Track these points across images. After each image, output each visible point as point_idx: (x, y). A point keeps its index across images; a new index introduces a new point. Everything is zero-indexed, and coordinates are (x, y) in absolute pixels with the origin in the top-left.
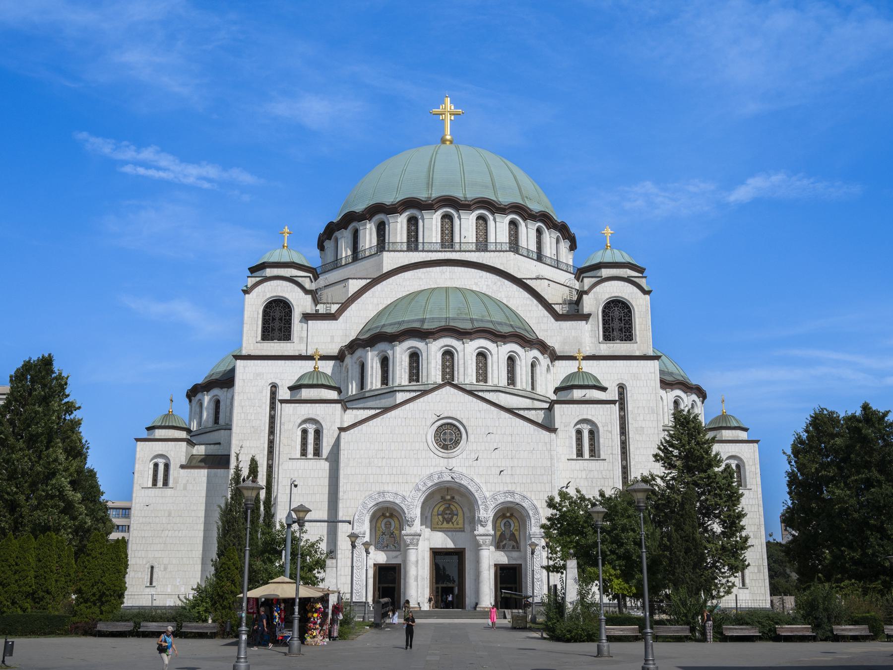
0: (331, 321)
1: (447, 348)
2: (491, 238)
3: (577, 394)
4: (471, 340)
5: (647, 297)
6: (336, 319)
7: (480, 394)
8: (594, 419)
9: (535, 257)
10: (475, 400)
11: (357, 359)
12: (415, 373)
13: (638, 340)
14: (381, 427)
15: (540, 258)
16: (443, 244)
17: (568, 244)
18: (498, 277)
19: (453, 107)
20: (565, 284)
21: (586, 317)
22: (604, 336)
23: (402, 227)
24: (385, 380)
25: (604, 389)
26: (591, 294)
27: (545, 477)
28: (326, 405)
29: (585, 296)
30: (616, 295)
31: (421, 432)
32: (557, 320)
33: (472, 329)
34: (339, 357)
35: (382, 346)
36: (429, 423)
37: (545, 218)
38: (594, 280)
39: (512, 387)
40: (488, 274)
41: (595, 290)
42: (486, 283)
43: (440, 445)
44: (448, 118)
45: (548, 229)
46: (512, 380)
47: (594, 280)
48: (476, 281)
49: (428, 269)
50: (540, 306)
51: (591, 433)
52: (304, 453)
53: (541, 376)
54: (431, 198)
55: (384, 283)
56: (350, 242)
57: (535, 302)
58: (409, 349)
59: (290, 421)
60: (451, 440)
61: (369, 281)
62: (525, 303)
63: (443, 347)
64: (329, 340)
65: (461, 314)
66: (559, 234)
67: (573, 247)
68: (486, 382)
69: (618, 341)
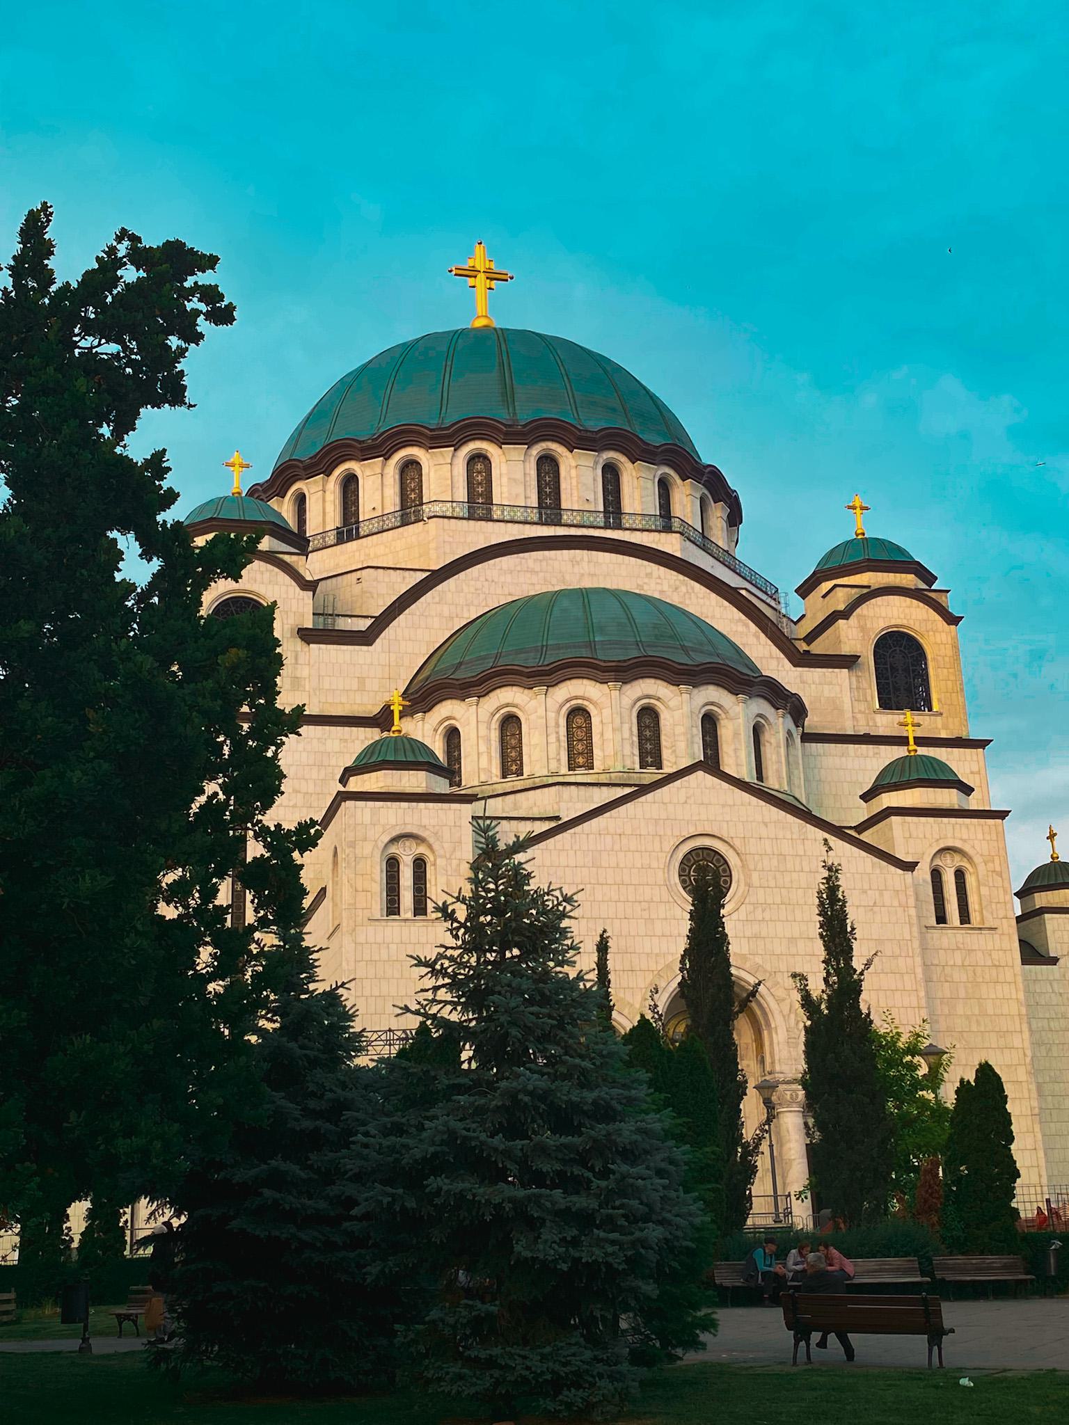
0: (357, 647)
8: (967, 848)
11: (441, 723)
14: (571, 853)
18: (681, 577)
21: (848, 662)
24: (511, 761)
26: (853, 619)
27: (901, 960)
28: (440, 804)
30: (899, 622)
31: (654, 865)
32: (796, 664)
33: (697, 666)
34: (380, 721)
35: (508, 697)
36: (669, 845)
40: (662, 568)
41: (858, 611)
42: (659, 588)
45: (715, 503)
47: (855, 593)
48: (640, 583)
49: (546, 553)
50: (762, 636)
51: (960, 875)
52: (393, 907)
53: (778, 771)
55: (462, 575)
56: (337, 502)
57: (753, 627)
58: (568, 701)
59: (365, 839)
62: (734, 629)
63: (639, 699)
64: (355, 687)
65: (662, 636)
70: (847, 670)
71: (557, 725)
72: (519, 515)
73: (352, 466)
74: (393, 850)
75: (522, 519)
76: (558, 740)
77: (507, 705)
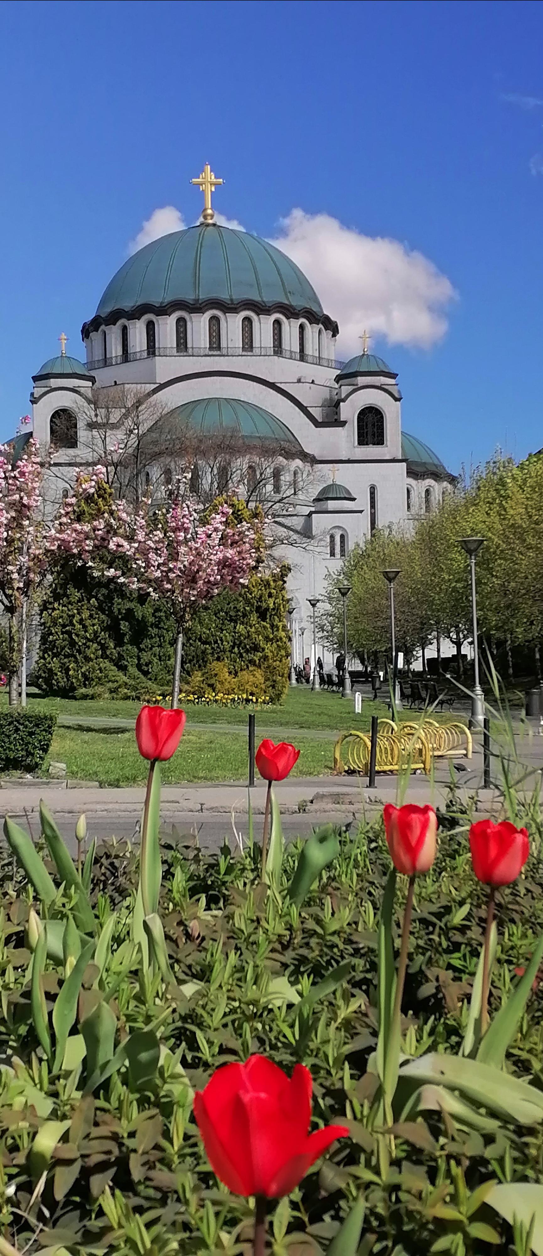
3: (332, 505)
5: (398, 403)
8: (344, 526)
9: (298, 357)
13: (389, 444)
16: (211, 348)
19: (213, 177)
21: (343, 424)
22: (358, 440)
23: (171, 329)
25: (354, 499)
29: (342, 404)
32: (316, 427)
38: (351, 388)
44: (209, 190)
47: (351, 388)
54: (198, 300)
57: (297, 408)
69: (371, 445)
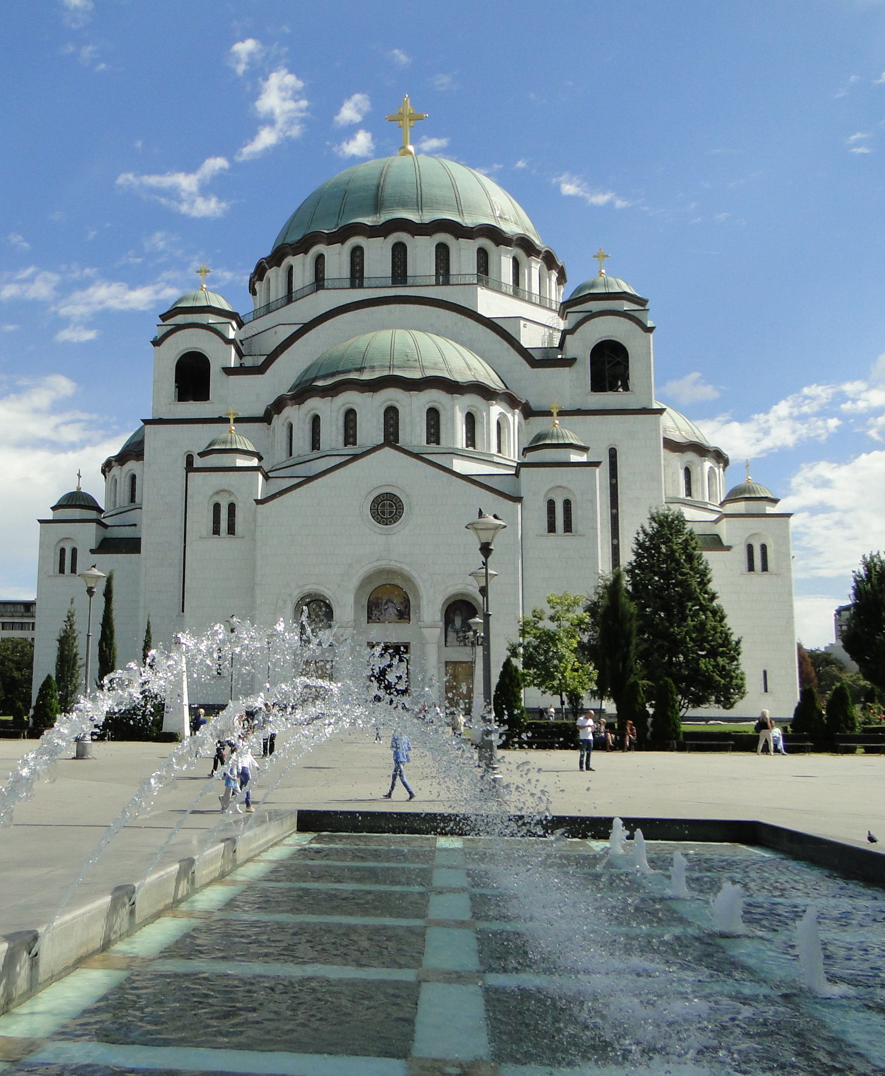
1: (389, 403)
2: (453, 270)
4: (420, 390)
6: (263, 373)
7: (424, 456)
9: (511, 292)
10: (420, 463)
12: (350, 436)
15: (517, 291)
17: (554, 275)
18: (459, 315)
20: (547, 324)
21: (569, 362)
24: (315, 444)
35: (315, 404)
37: (526, 245)
39: (471, 449)
40: (447, 311)
43: (378, 518)
46: (471, 440)
49: (372, 309)
50: (512, 351)
52: (216, 531)
55: (319, 327)
57: (506, 345)
58: (343, 405)
60: (391, 513)
61: (301, 325)
66: (543, 264)
67: (562, 279)
68: (438, 443)
70: (568, 368)
71: (337, 419)
72: (378, 283)
73: (289, 260)
74: (217, 499)
75: (375, 285)
76: (337, 428)
77: (312, 410)
